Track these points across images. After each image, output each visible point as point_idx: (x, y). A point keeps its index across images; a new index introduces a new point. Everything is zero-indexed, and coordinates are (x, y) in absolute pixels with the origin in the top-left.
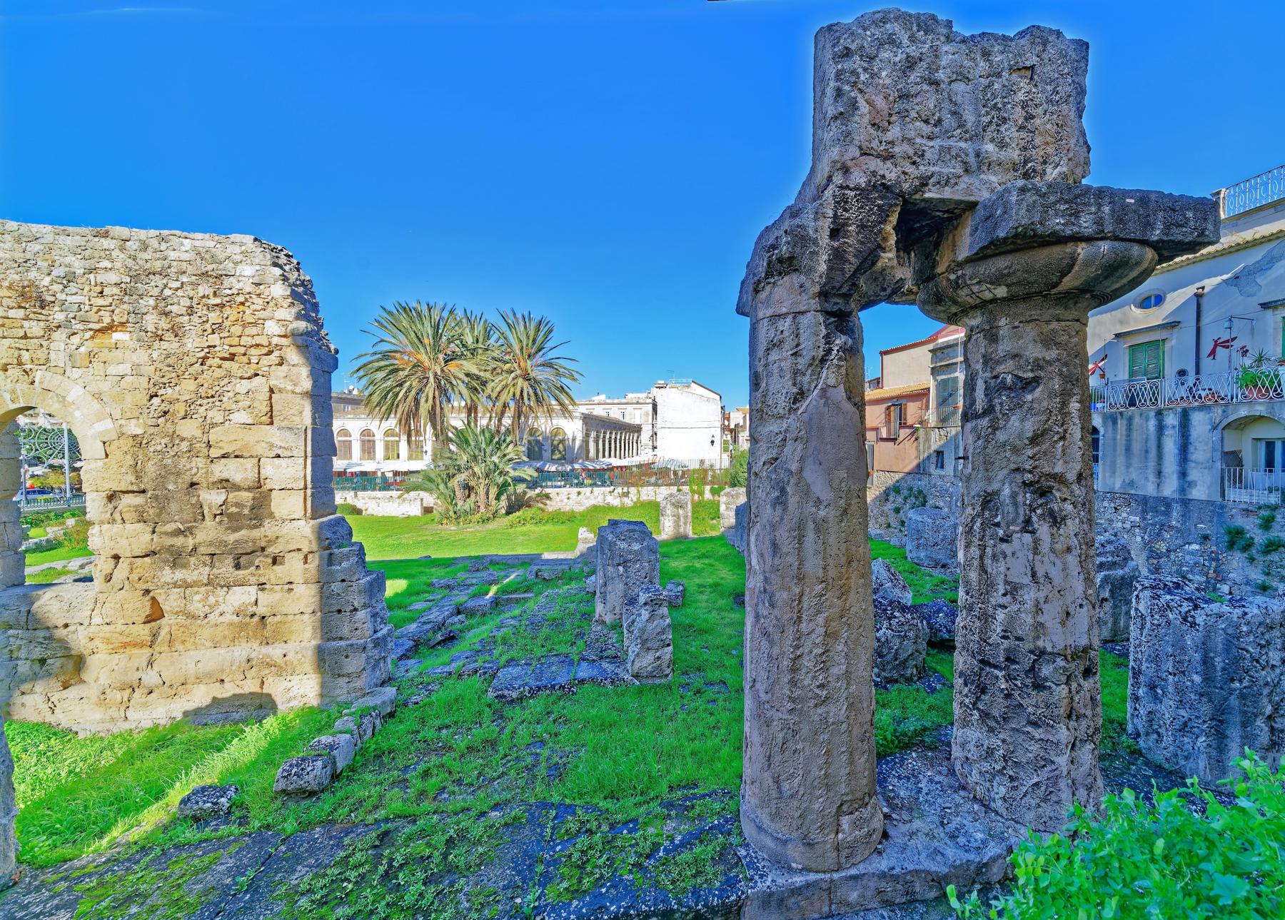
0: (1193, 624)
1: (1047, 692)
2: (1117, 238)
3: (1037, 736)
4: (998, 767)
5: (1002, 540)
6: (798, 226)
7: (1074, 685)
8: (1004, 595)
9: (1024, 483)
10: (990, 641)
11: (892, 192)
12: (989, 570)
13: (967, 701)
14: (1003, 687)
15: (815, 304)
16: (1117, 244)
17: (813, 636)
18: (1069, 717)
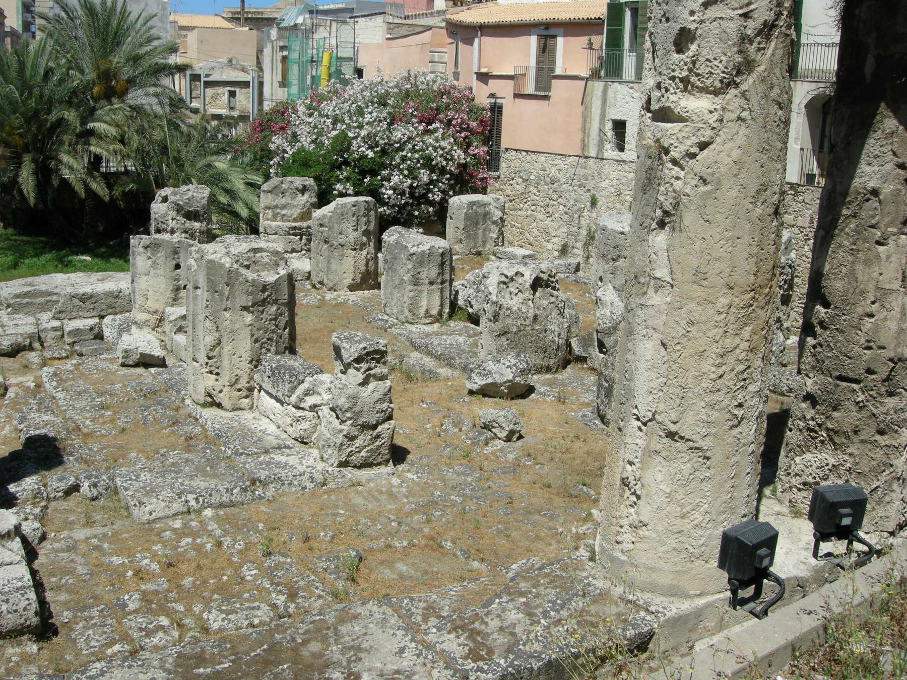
3: (883, 443)
5: (879, 243)
8: (873, 303)
12: (860, 277)
13: (811, 423)
14: (860, 399)
17: (738, 351)
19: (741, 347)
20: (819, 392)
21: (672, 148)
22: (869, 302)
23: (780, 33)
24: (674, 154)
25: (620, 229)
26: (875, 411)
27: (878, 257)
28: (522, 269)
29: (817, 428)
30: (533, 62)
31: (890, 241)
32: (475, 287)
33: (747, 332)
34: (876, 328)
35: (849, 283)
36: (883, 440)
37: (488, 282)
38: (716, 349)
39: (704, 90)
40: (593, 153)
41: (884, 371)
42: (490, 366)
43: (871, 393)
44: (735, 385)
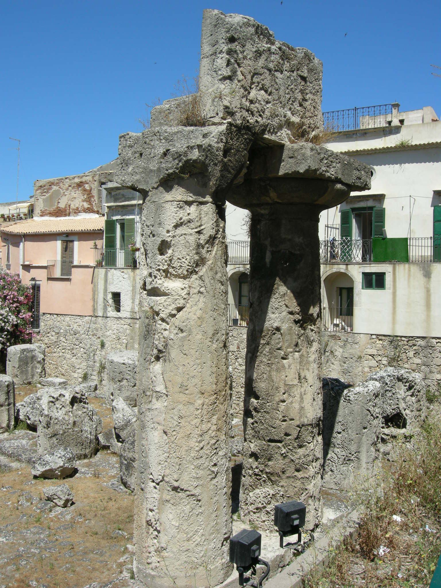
1: (304, 448)
3: (300, 477)
5: (283, 358)
8: (284, 394)
12: (275, 380)
13: (256, 470)
14: (283, 452)
17: (210, 432)
19: (212, 429)
20: (259, 451)
21: (161, 312)
22: (281, 394)
23: (219, 241)
24: (162, 315)
25: (123, 362)
26: (293, 458)
27: (283, 366)
28: (63, 392)
29: (260, 473)
30: (59, 258)
31: (289, 357)
32: (31, 406)
33: (214, 419)
34: (288, 408)
35: (269, 383)
36: (299, 475)
37: (41, 402)
38: (198, 432)
39: (178, 276)
40: (100, 313)
41: (294, 433)
42: (48, 458)
43: (289, 447)
44: (211, 453)
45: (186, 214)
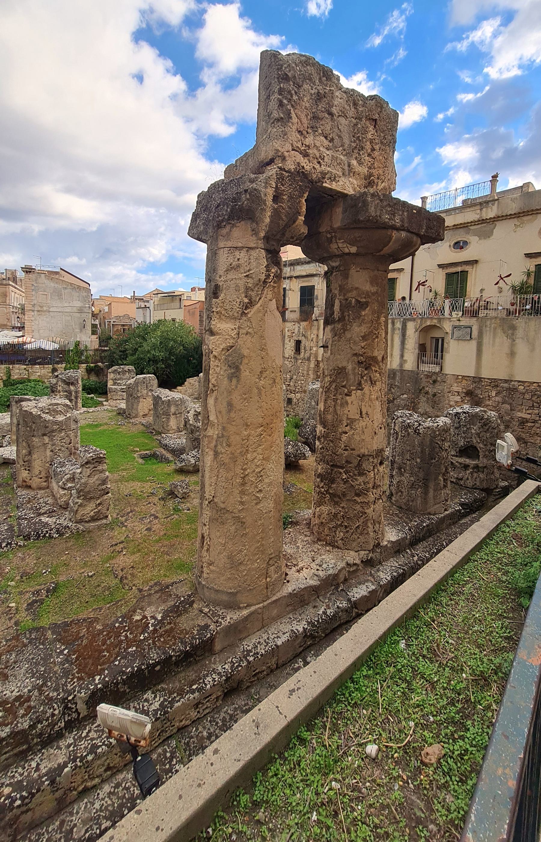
0: (419, 434)
2: (408, 231)
3: (359, 501)
4: (339, 523)
5: (346, 395)
6: (255, 190)
7: (376, 470)
8: (346, 426)
9: (359, 362)
10: (338, 453)
11: (307, 178)
15: (261, 244)
16: (408, 234)
18: (373, 488)
41: (355, 462)
45: (236, 259)
